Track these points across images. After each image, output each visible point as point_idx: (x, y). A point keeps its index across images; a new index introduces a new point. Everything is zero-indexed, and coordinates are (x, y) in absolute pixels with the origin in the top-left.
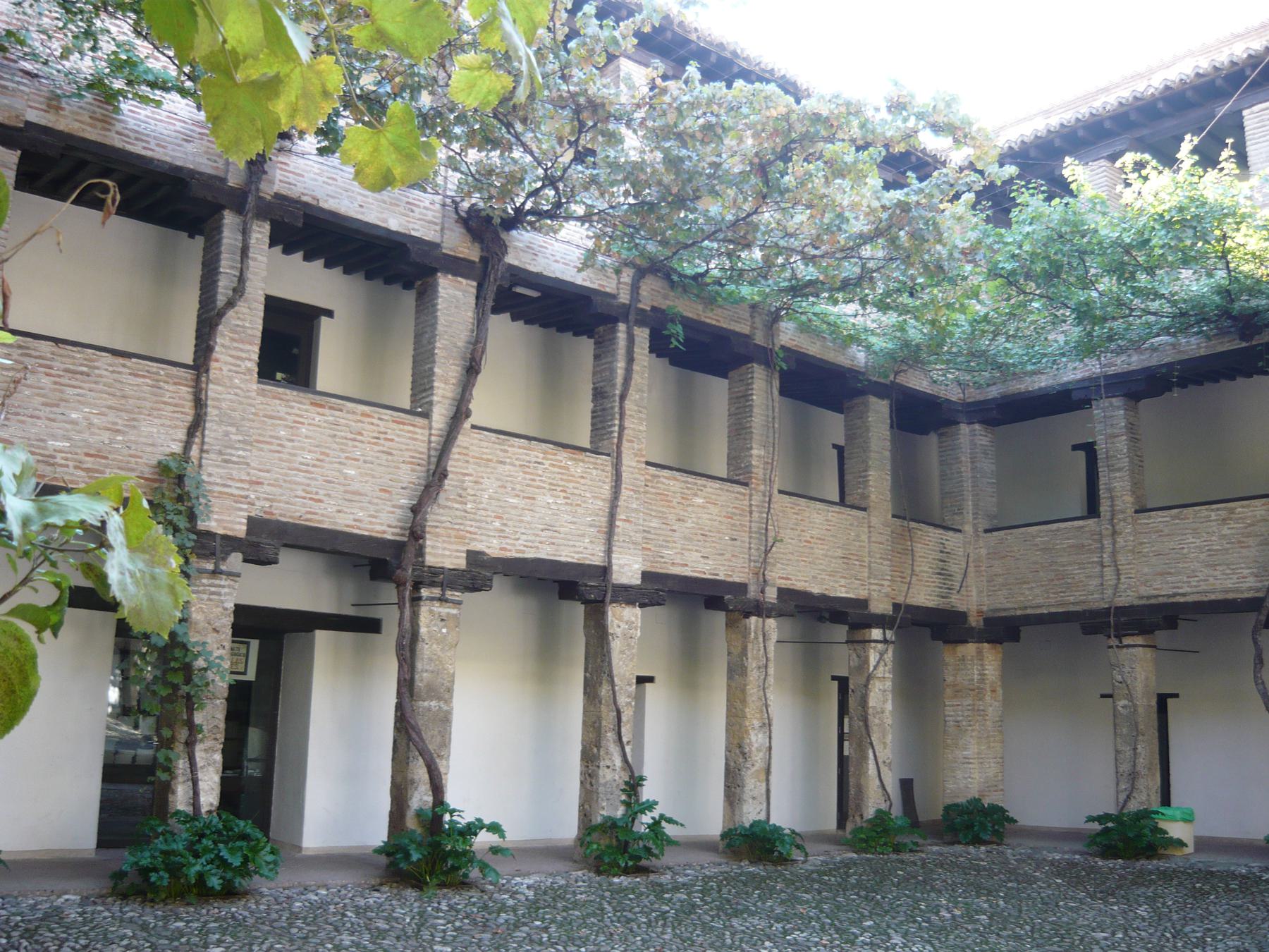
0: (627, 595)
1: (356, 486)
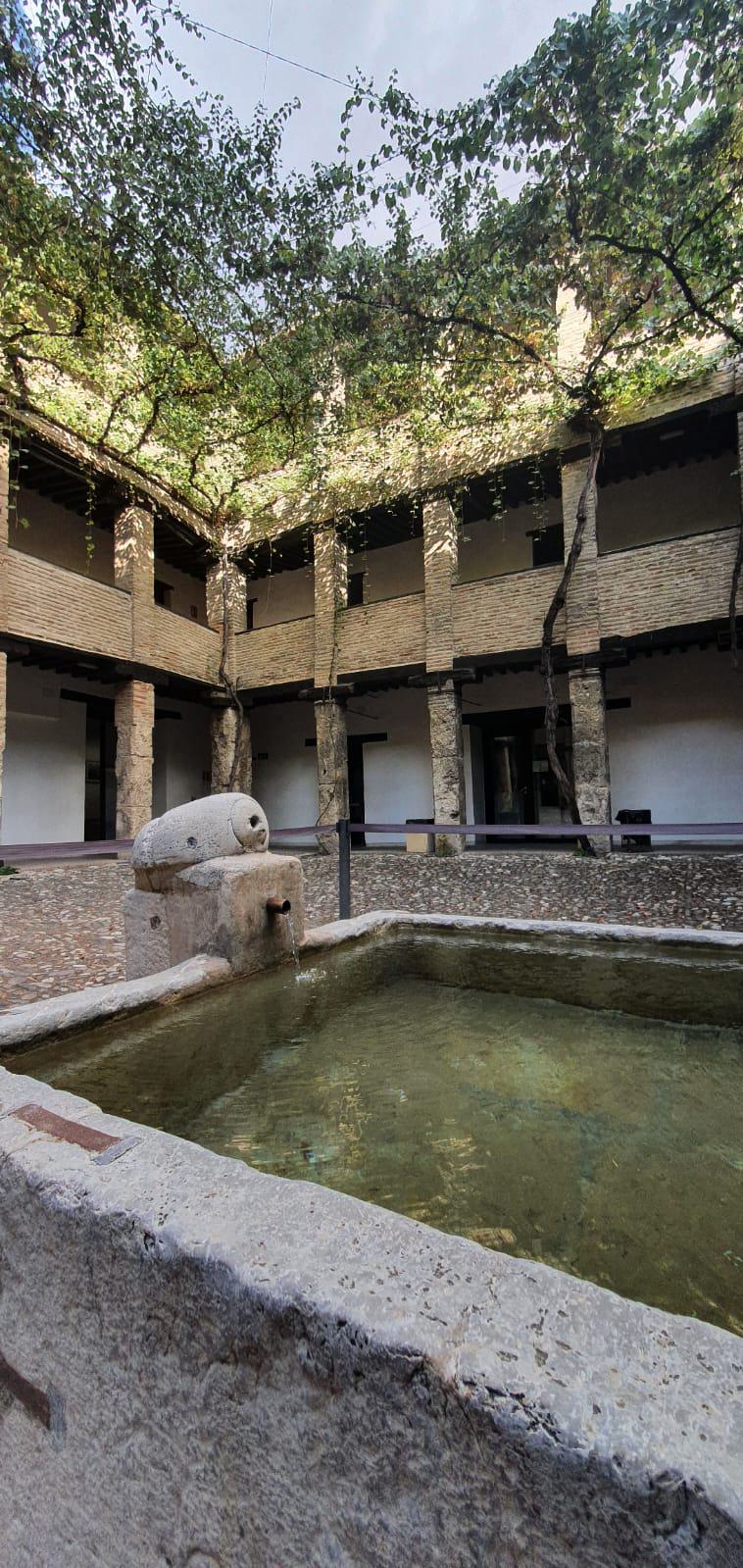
1: (518, 623)
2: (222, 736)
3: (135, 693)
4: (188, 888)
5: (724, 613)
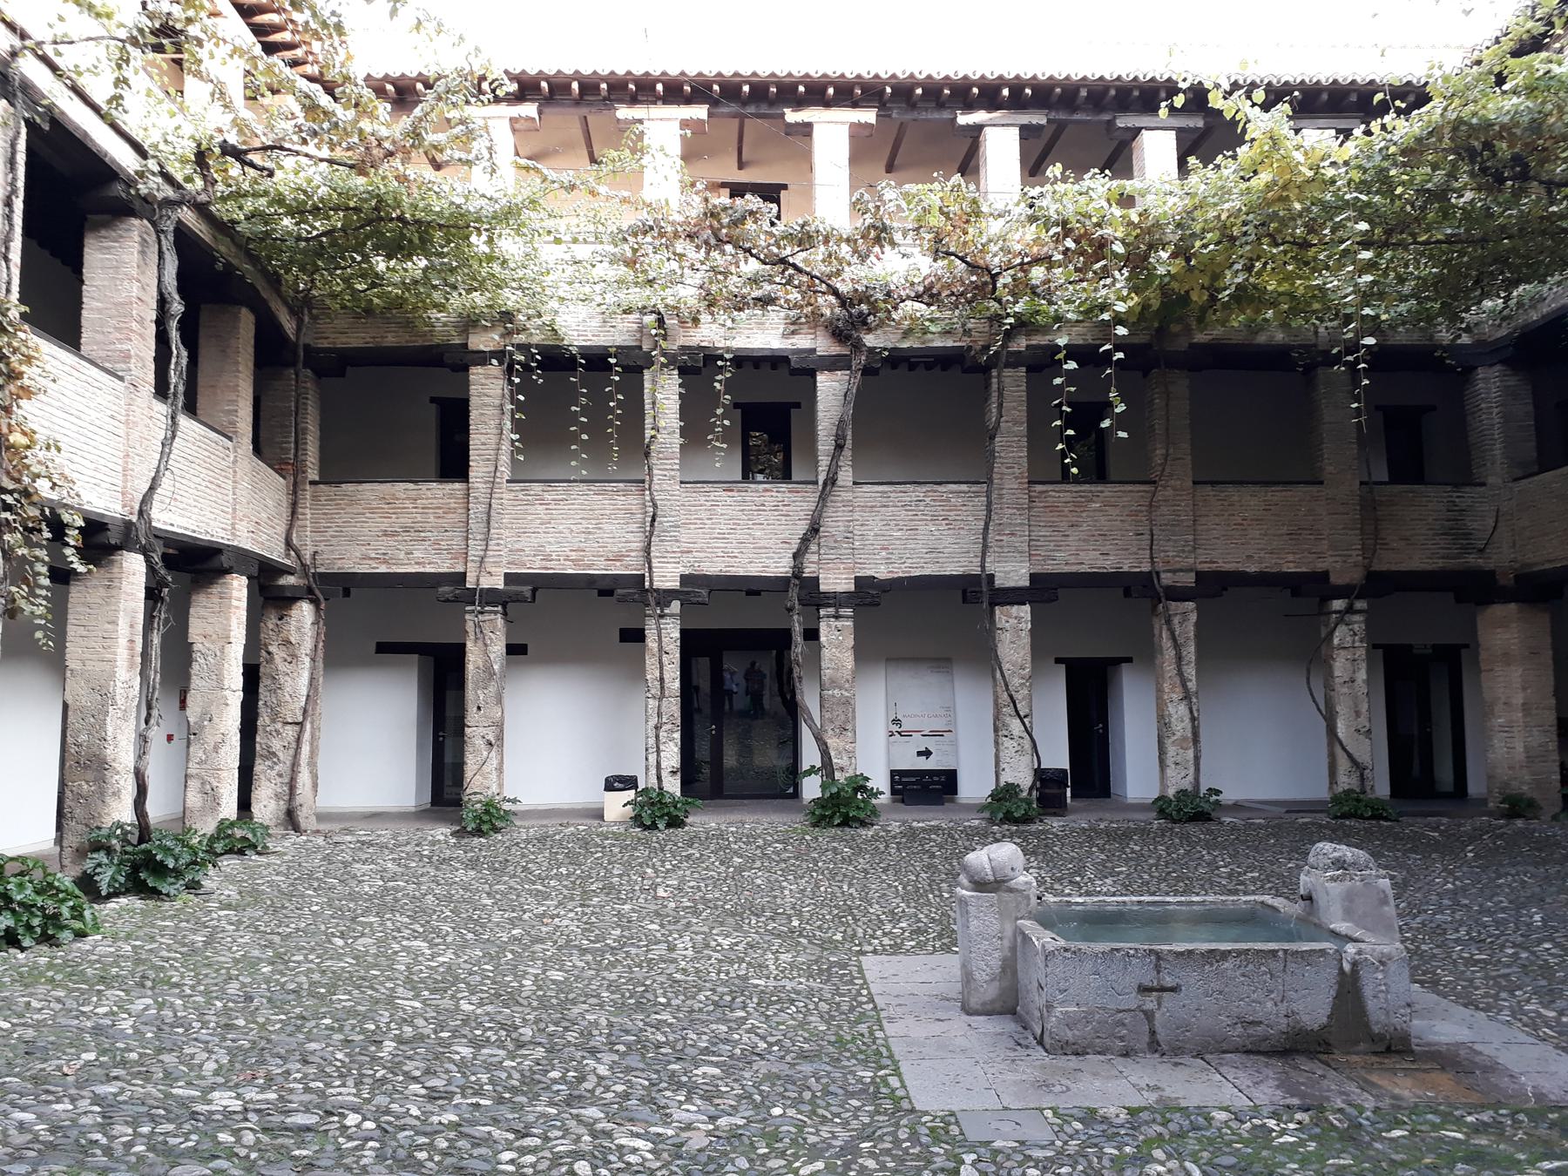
0: (1013, 596)
1: (762, 543)
2: (287, 642)
3: (235, 594)
4: (1011, 890)
5: (977, 571)
